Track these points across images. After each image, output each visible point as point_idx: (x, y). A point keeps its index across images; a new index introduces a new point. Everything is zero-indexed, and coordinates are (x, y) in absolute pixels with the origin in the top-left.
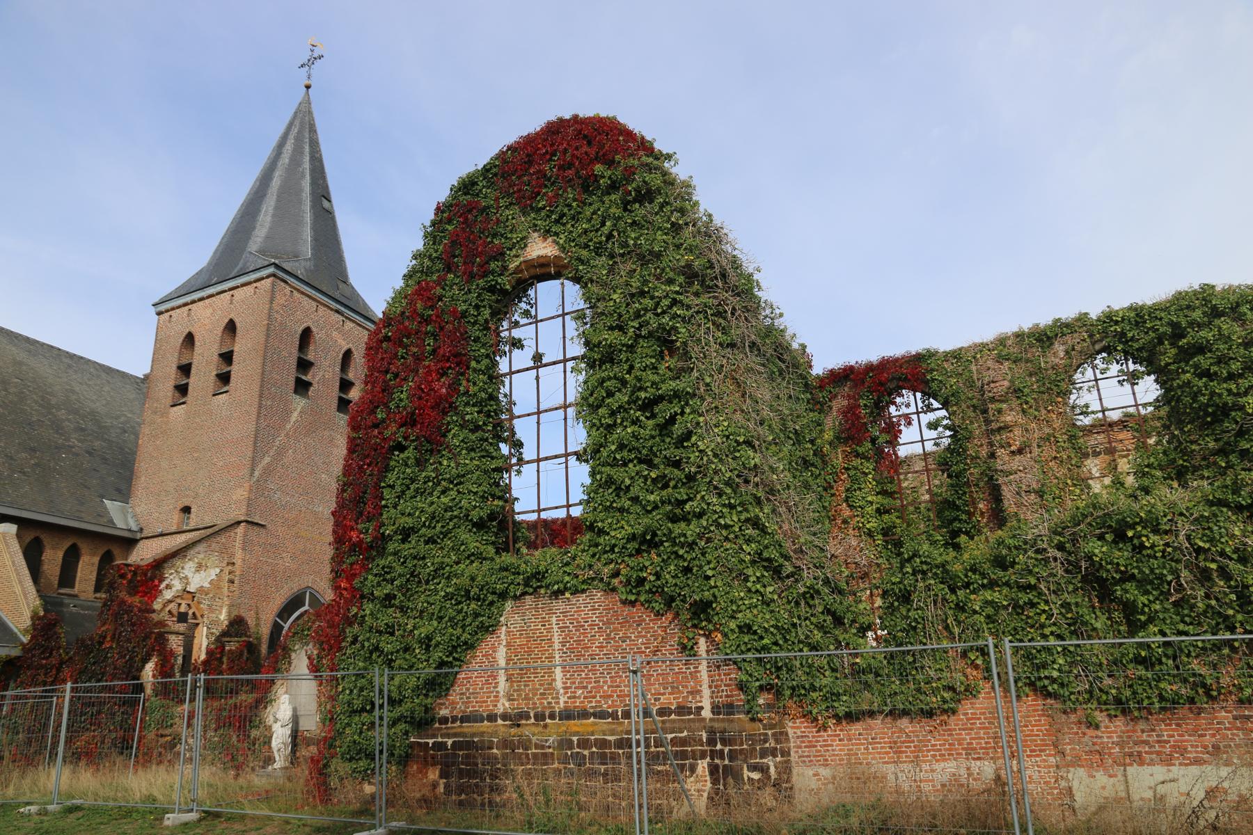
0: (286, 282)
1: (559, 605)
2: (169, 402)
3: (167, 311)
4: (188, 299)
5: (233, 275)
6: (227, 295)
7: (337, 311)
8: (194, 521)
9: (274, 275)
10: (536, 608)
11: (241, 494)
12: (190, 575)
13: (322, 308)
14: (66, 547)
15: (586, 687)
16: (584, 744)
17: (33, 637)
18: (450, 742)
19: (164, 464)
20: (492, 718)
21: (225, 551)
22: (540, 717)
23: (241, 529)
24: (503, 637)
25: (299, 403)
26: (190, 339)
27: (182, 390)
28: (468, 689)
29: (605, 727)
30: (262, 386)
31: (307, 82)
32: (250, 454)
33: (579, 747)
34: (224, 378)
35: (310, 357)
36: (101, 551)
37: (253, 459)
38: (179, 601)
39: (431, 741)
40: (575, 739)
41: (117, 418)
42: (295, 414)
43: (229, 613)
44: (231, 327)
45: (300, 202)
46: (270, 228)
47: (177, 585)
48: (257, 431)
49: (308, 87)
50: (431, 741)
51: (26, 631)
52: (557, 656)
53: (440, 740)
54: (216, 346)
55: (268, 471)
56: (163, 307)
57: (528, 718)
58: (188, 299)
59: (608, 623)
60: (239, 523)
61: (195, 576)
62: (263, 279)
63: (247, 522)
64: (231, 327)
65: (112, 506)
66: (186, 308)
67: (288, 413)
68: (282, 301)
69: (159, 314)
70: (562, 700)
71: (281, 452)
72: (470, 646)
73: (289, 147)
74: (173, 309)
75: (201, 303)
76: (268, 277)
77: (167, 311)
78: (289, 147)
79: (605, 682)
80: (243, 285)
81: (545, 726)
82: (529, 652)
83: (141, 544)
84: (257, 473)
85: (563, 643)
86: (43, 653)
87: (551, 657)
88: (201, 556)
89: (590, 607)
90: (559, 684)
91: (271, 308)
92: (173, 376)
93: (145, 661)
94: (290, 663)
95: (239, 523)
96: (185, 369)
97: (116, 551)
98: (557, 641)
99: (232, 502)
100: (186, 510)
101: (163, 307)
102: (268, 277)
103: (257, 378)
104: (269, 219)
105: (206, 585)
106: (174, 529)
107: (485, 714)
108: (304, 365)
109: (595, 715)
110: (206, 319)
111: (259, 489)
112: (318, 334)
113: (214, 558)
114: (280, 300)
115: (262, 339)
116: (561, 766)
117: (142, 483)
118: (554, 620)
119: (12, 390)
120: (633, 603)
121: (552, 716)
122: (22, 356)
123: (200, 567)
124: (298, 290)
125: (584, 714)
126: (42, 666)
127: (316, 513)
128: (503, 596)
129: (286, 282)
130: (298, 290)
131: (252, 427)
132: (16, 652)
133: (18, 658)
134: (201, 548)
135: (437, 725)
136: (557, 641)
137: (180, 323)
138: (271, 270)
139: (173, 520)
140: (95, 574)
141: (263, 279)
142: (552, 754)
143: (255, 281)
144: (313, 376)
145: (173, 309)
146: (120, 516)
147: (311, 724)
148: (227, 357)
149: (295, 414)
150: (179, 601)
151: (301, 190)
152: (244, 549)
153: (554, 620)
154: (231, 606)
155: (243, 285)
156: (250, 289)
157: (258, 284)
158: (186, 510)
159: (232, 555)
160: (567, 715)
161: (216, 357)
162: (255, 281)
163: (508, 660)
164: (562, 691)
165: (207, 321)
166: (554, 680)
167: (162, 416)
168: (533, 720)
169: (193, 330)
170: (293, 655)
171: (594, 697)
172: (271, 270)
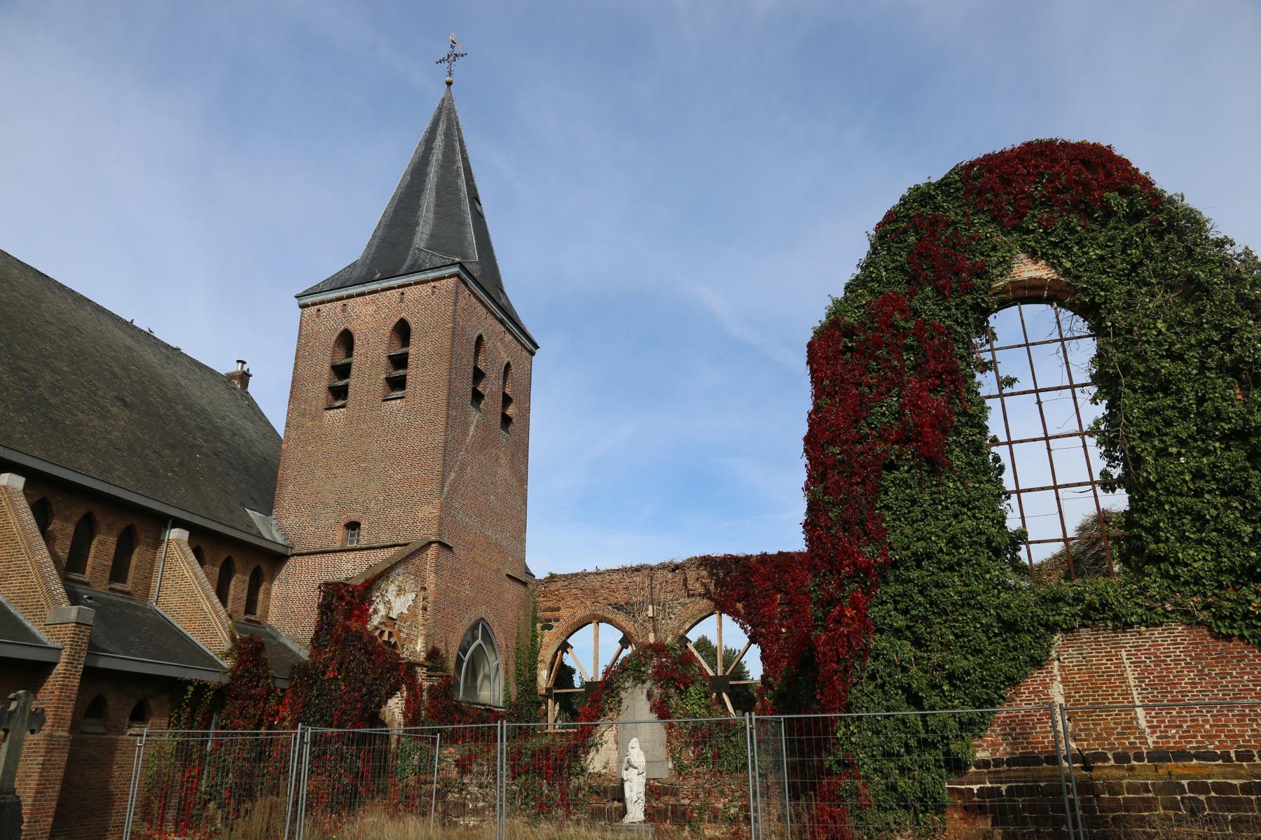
0: (466, 284)
1: (1128, 639)
2: (322, 403)
3: (314, 304)
4: (343, 293)
5: (402, 271)
6: (396, 293)
7: (501, 322)
8: (365, 538)
9: (457, 275)
10: (1096, 641)
11: (430, 511)
12: (393, 599)
13: (490, 317)
14: (221, 562)
15: (1181, 726)
16: (1197, 787)
17: (240, 662)
18: (1004, 787)
19: (320, 473)
20: (1053, 759)
21: (419, 575)
22: (1121, 758)
23: (432, 551)
24: (1056, 672)
25: (475, 416)
26: (346, 340)
27: (339, 393)
28: (1014, 729)
29: (1217, 770)
30: (449, 394)
31: (448, 79)
32: (438, 468)
33: (1191, 791)
34: (397, 384)
35: (481, 366)
36: (252, 568)
37: (443, 472)
38: (383, 628)
39: (975, 788)
40: (1185, 782)
41: (223, 418)
42: (472, 428)
43: (426, 643)
44: (403, 331)
45: (459, 201)
46: (434, 226)
47: (382, 611)
48: (446, 442)
49: (449, 84)
50: (975, 788)
51: (226, 655)
52: (1135, 693)
53: (989, 785)
54: (384, 347)
55: (454, 488)
56: (308, 299)
57: (1106, 759)
58: (343, 293)
59: (1198, 658)
60: (431, 543)
61: (396, 601)
62: (444, 278)
63: (440, 543)
64: (403, 331)
65: (255, 515)
66: (340, 303)
67: (467, 425)
68: (462, 305)
69: (303, 307)
70: (1150, 741)
71: (462, 469)
72: (1012, 681)
73: (439, 142)
74: (322, 302)
75: (360, 299)
76: (450, 277)
77: (314, 304)
78: (439, 142)
79: (1207, 721)
80: (417, 283)
81: (1132, 769)
82: (1095, 688)
83: (292, 561)
84: (446, 489)
85: (1141, 679)
86: (251, 681)
87: (1126, 694)
88: (401, 578)
89: (1171, 641)
90: (1143, 723)
91: (455, 311)
92: (326, 376)
93: (391, 694)
94: (620, 702)
95: (431, 543)
96: (342, 371)
97: (265, 568)
98: (1131, 677)
99: (423, 519)
100: (353, 526)
101: (308, 299)
102: (450, 277)
103: (443, 386)
104: (431, 215)
105: (405, 611)
106: (337, 546)
107: (1043, 756)
108: (478, 375)
109: (1198, 756)
110: (370, 316)
111: (446, 508)
112: (488, 344)
113: (410, 584)
114: (462, 304)
115: (447, 344)
116: (1171, 813)
117: (287, 494)
118: (1124, 654)
119: (134, 378)
120: (1228, 638)
121: (1139, 757)
122: (129, 341)
123: (400, 591)
124: (475, 295)
125: (1182, 755)
126: (251, 697)
127: (487, 538)
128: (1052, 628)
129: (466, 284)
130: (475, 295)
131: (439, 438)
132: (226, 680)
133: (228, 685)
134: (400, 570)
135: (973, 769)
136: (1131, 677)
137: (332, 319)
138: (456, 269)
139: (338, 537)
140: (246, 592)
141: (444, 278)
142: (1155, 799)
143: (433, 280)
144: (485, 388)
145: (322, 302)
146: (271, 529)
147: (665, 771)
148: (400, 361)
149: (472, 428)
150: (383, 628)
151: (459, 190)
152: (436, 573)
153: (1124, 654)
154: (427, 636)
155: (417, 283)
156: (427, 288)
157: (437, 284)
158: (353, 526)
159: (424, 580)
160: (1158, 756)
161: (384, 360)
162: (433, 280)
163: (1067, 697)
164: (1148, 731)
165: (369, 319)
166: (1136, 718)
167: (313, 419)
168: (1112, 762)
169: (350, 328)
170: (623, 694)
171: (1195, 737)
172: (456, 269)
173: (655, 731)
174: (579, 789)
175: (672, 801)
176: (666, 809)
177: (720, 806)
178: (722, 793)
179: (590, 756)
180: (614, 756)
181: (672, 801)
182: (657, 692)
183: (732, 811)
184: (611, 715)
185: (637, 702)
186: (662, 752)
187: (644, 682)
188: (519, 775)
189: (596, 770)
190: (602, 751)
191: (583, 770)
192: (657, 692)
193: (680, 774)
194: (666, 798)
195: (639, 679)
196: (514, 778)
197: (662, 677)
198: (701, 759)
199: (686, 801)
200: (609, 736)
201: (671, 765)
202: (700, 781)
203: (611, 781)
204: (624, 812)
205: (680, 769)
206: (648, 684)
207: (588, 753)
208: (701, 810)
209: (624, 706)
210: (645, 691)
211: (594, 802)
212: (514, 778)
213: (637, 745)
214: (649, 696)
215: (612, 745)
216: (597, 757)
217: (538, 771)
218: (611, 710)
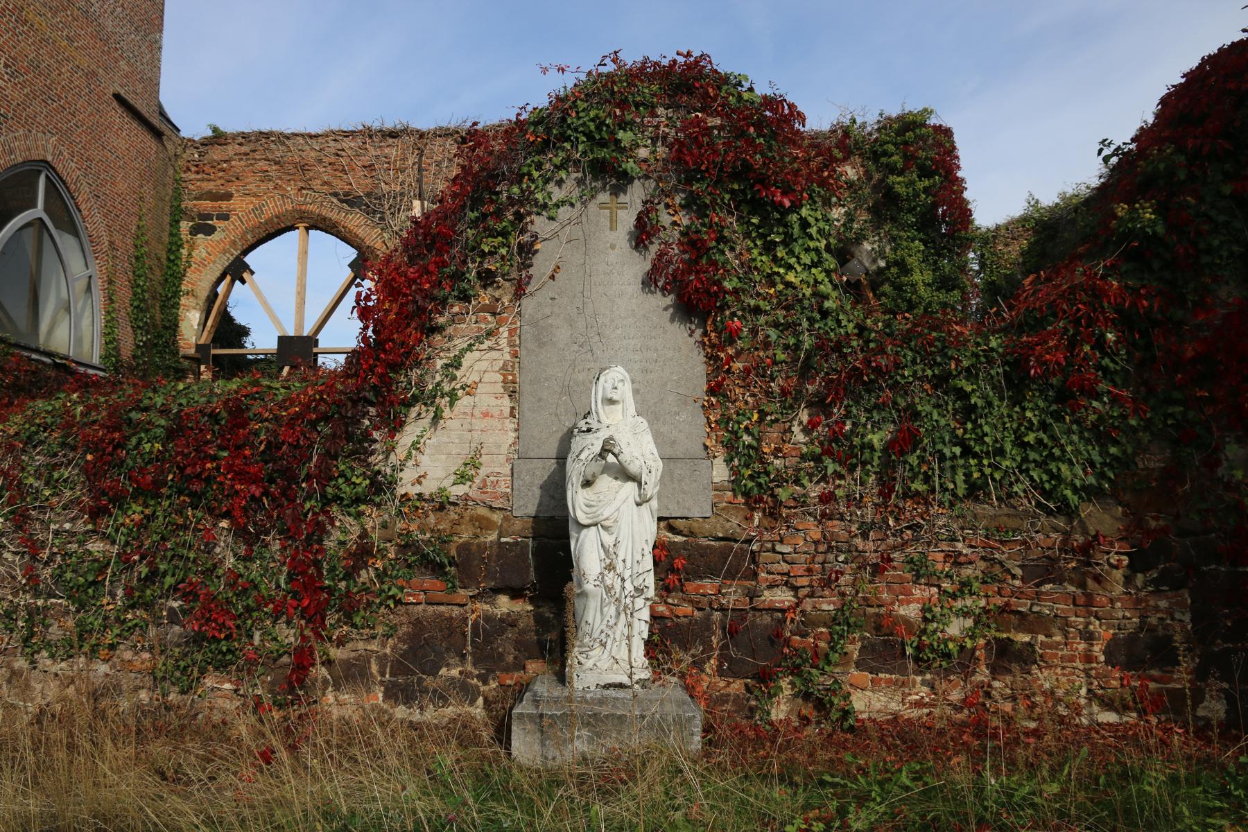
173: (681, 352)
174: (363, 552)
175: (733, 595)
176: (706, 624)
177: (911, 611)
178: (920, 571)
179: (405, 439)
180: (499, 440)
181: (733, 595)
182: (673, 221)
183: (955, 628)
184: (485, 297)
185: (594, 257)
186: (692, 427)
187: (621, 182)
188: (119, 500)
189: (428, 488)
190: (453, 420)
191: (380, 486)
192: (673, 221)
193: (752, 501)
194: (708, 586)
195: (609, 174)
196: (96, 513)
197: (689, 164)
198: (840, 450)
199: (783, 597)
200: (482, 367)
201: (720, 472)
202: (835, 526)
203: (483, 524)
204: (554, 638)
205: (756, 490)
206: (636, 195)
207: (396, 426)
208: (840, 622)
209: (541, 265)
210: (627, 219)
211: (421, 598)
212: (96, 513)
213: (625, 392)
214: (643, 233)
215: (490, 396)
216: (433, 441)
217: (195, 488)
218: (487, 278)
